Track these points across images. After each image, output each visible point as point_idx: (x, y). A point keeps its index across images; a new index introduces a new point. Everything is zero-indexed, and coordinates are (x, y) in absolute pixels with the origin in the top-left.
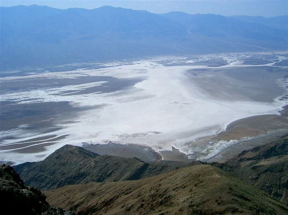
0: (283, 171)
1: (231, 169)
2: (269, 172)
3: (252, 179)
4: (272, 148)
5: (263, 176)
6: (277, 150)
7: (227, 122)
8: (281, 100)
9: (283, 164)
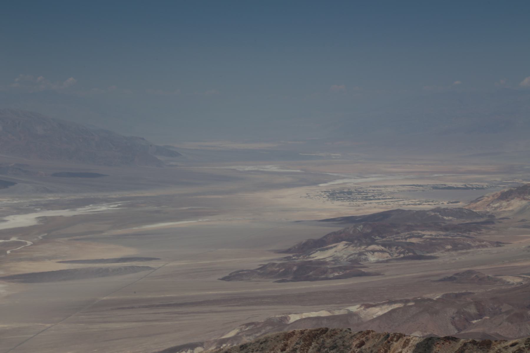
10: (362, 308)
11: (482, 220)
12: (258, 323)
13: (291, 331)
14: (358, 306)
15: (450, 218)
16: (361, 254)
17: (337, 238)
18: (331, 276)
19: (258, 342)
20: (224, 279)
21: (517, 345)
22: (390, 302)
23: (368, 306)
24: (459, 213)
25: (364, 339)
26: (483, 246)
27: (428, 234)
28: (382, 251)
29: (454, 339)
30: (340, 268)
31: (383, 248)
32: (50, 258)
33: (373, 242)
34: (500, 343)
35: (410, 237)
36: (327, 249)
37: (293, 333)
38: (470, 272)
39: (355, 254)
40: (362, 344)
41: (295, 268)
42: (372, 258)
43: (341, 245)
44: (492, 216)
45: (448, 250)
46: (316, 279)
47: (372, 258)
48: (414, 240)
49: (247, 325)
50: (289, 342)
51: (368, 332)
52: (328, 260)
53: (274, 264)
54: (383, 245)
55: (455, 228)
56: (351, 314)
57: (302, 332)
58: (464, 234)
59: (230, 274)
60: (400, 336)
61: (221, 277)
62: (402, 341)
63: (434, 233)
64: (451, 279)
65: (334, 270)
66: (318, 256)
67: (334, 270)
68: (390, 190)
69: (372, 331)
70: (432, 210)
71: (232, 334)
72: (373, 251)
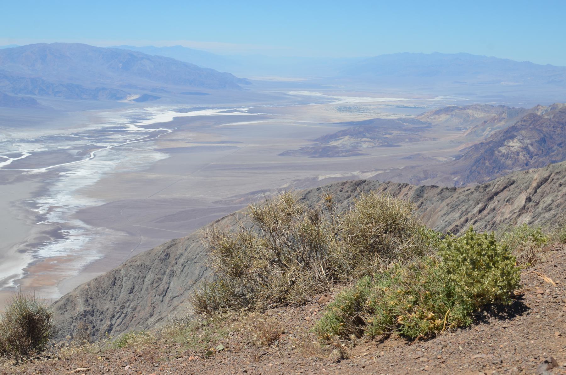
8: (22, 251)
10: (360, 173)
12: (301, 180)
13: (345, 181)
14: (358, 172)
15: (407, 124)
16: (358, 143)
17: (344, 133)
18: (341, 155)
19: (327, 186)
21: (470, 190)
23: (363, 172)
24: (412, 121)
25: (386, 186)
26: (426, 140)
27: (395, 132)
28: (370, 142)
29: (437, 187)
30: (346, 151)
31: (371, 140)
32: (182, 140)
33: (364, 136)
34: (461, 189)
35: (385, 134)
36: (339, 140)
37: (347, 182)
38: (419, 155)
39: (355, 143)
40: (386, 189)
41: (320, 150)
43: (347, 138)
44: (430, 124)
45: (407, 142)
46: (332, 156)
47: (365, 146)
48: (387, 136)
49: (295, 181)
50: (344, 187)
52: (339, 146)
53: (308, 147)
54: (371, 138)
55: (411, 130)
56: (354, 176)
57: (351, 182)
58: (415, 133)
59: (283, 152)
60: (407, 185)
61: (278, 154)
62: (408, 187)
63: (399, 132)
64: (409, 158)
65: (342, 152)
66: (333, 143)
67: (342, 152)
68: (372, 107)
69: (391, 182)
70: (398, 119)
72: (365, 142)
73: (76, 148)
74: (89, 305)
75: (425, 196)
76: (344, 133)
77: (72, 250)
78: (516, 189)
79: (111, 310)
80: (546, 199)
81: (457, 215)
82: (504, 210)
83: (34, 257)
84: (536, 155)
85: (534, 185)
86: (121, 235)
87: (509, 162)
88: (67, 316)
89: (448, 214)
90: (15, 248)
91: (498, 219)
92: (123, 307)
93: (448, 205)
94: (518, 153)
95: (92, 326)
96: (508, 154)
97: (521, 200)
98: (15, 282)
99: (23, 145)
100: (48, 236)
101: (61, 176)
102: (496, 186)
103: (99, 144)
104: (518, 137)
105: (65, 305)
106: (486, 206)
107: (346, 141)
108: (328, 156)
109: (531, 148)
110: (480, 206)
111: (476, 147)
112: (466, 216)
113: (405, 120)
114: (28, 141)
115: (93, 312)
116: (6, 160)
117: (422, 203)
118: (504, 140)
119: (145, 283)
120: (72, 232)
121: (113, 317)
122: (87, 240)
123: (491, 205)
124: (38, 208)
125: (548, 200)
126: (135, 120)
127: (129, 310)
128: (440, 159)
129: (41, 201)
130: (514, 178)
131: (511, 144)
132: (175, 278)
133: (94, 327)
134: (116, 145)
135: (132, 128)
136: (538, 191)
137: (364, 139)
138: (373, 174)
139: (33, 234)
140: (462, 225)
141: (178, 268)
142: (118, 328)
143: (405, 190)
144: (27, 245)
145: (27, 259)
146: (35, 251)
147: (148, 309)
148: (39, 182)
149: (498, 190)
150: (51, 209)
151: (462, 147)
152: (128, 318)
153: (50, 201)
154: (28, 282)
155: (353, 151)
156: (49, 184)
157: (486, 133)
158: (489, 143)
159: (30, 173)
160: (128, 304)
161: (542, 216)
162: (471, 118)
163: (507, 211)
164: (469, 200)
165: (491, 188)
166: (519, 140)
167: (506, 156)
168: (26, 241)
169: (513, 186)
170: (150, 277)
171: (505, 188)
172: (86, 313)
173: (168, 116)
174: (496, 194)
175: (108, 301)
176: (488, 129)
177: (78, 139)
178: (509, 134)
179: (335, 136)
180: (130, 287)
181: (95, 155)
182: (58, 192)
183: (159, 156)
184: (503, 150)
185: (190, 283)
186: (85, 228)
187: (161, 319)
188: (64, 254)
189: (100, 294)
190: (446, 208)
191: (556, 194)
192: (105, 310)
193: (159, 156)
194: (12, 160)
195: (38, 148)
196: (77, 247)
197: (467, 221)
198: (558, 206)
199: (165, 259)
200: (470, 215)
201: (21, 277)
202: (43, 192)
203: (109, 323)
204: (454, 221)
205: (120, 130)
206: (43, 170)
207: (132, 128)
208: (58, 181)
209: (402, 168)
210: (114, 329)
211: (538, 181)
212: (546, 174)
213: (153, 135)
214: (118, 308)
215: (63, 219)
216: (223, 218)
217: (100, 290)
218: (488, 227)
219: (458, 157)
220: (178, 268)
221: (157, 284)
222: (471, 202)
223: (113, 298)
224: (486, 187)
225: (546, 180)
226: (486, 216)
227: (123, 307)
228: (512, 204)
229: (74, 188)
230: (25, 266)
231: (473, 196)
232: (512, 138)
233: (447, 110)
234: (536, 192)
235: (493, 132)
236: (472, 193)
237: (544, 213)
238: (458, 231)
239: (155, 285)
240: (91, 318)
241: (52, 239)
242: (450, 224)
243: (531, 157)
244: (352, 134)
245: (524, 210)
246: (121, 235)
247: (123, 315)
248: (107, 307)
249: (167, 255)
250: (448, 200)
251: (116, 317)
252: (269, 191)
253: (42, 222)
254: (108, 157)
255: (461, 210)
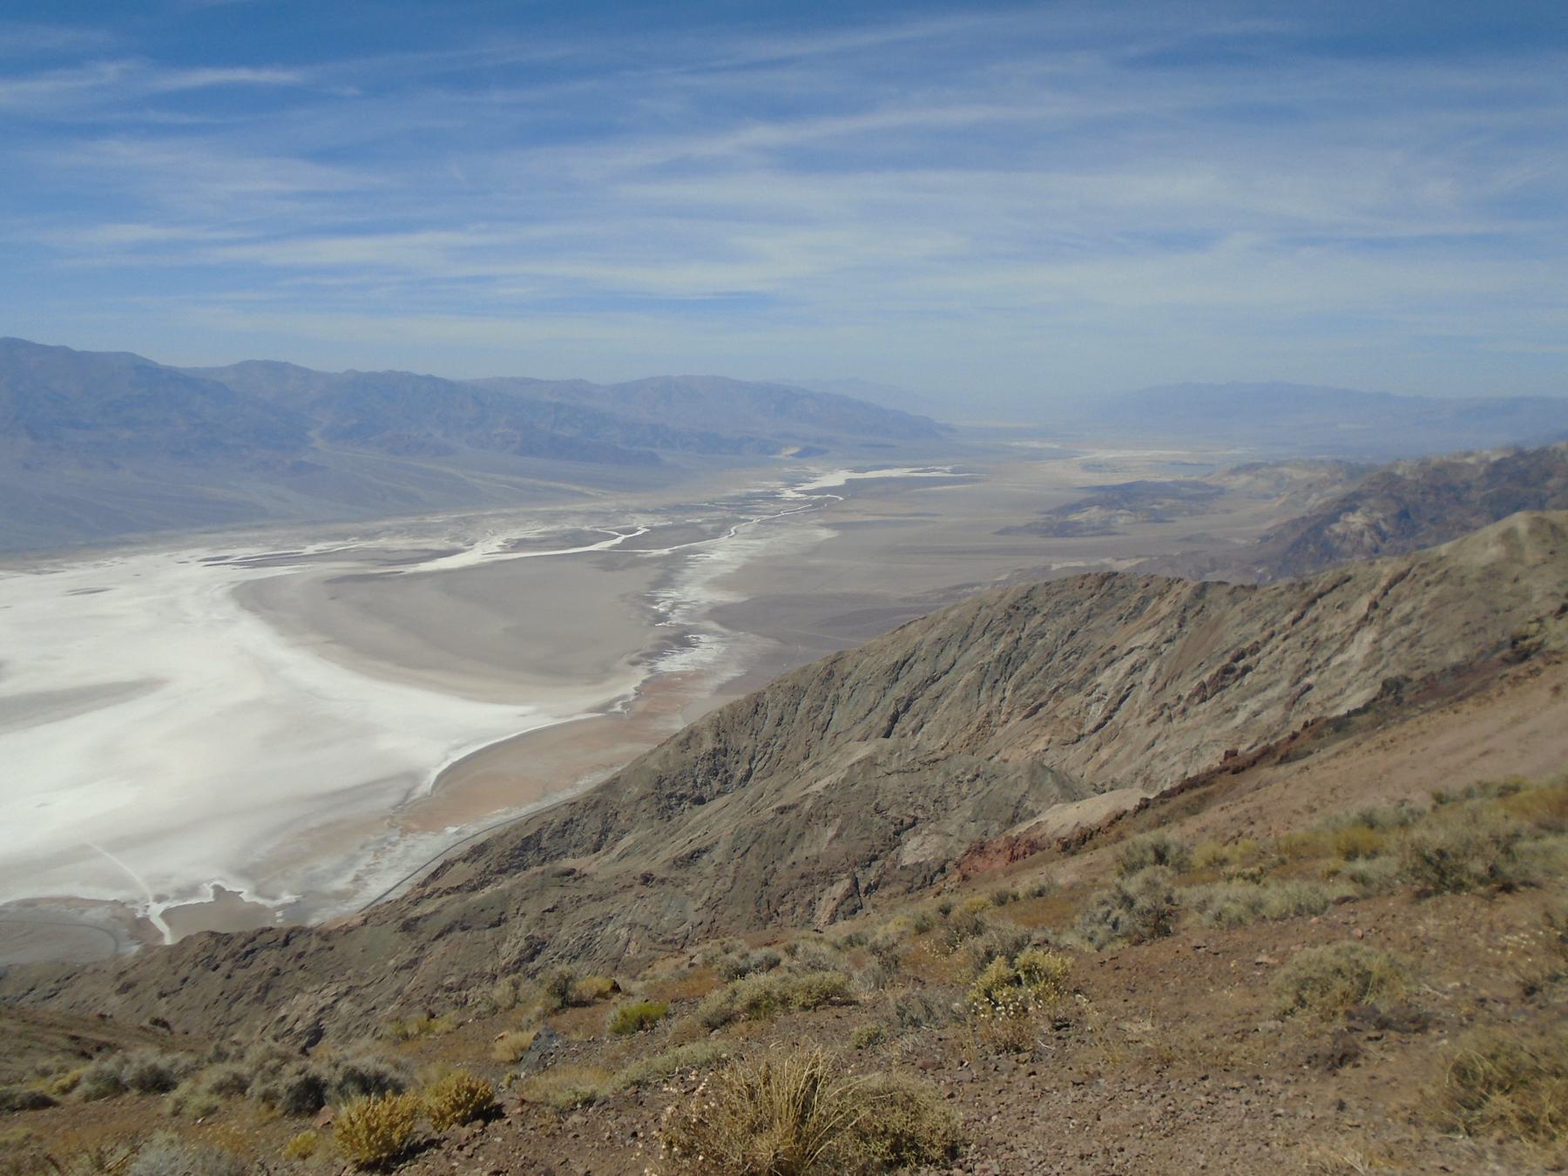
0: (505, 920)
1: (323, 944)
2: (457, 934)
3: (398, 969)
4: (528, 839)
5: (440, 947)
6: (544, 844)
7: (439, 765)
8: (634, 663)
9: (506, 898)
11: (1211, 491)
17: (1090, 503)
20: (995, 533)
22: (1138, 557)
23: (1118, 560)
24: (1195, 485)
27: (1168, 502)
29: (1225, 583)
30: (1094, 528)
33: (1121, 507)
37: (1089, 574)
40: (1147, 585)
42: (1121, 521)
43: (1094, 509)
47: (1121, 521)
48: (1156, 506)
49: (1017, 570)
51: (1152, 577)
56: (1103, 566)
62: (1181, 584)
64: (1189, 540)
70: (1174, 483)
71: (1004, 577)
72: (1121, 515)
73: (710, 522)
74: (720, 741)
75: (1208, 596)
76: (1090, 503)
77: (702, 663)
78: (1354, 590)
79: (750, 749)
80: (1402, 605)
81: (1258, 626)
82: (1332, 621)
83: (651, 671)
84: (1392, 536)
85: (1384, 583)
86: (770, 644)
87: (1347, 547)
88: (690, 754)
89: (1244, 625)
90: (625, 659)
91: (1323, 634)
92: (767, 745)
93: (1243, 611)
94: (1362, 534)
95: (723, 770)
96: (1345, 535)
97: (1361, 606)
98: (624, 706)
99: (638, 517)
100: (669, 642)
101: (689, 560)
102: (1320, 585)
103: (742, 517)
104: (1363, 509)
105: (688, 739)
106: (1302, 615)
107: (1094, 514)
108: (1066, 535)
109: (1384, 527)
110: (1294, 613)
111: (1294, 524)
112: (1271, 629)
113: (1182, 484)
114: (646, 512)
115: (726, 750)
116: (616, 537)
117: (1203, 607)
118: (1340, 513)
119: (799, 712)
120: (702, 638)
121: (753, 758)
122: (724, 648)
123: (1311, 614)
124: (658, 603)
125: (1406, 607)
126: (792, 483)
127: (776, 749)
128: (1237, 541)
129: (663, 594)
130: (1350, 573)
131: (1351, 519)
132: (841, 706)
133: (726, 771)
134: (765, 517)
135: (789, 494)
136: (1390, 592)
137: (1121, 511)
138: (1134, 562)
139: (650, 639)
140: (1266, 642)
141: (845, 692)
142: (760, 775)
143: (1177, 588)
144: (641, 655)
145: (641, 674)
146: (652, 664)
147: (802, 749)
148: (659, 568)
149: (1325, 590)
150: (674, 606)
151: (1271, 523)
152: (774, 759)
153: (674, 594)
154: (640, 706)
155: (1104, 529)
156: (673, 571)
157: (1311, 502)
158: (1316, 517)
159: (646, 556)
160: (774, 740)
161: (1396, 631)
162: (1287, 480)
163: (1336, 624)
164: (1277, 604)
165: (1313, 586)
166: (1365, 514)
167: (1344, 538)
168: (638, 651)
169: (1348, 584)
170: (805, 703)
171: (1335, 587)
172: (715, 753)
173: (838, 478)
174: (1321, 595)
175: (746, 736)
176: (1315, 496)
177: (714, 510)
178: (1349, 504)
179: (1077, 507)
180: (777, 717)
181: (735, 531)
182: (686, 582)
183: (825, 534)
184: (1338, 528)
185: (862, 714)
186: (722, 633)
187: (818, 764)
188: (691, 668)
189: (736, 725)
190: (1240, 616)
191: (1420, 597)
192: (742, 748)
193: (825, 534)
194: (623, 537)
195: (659, 522)
196: (708, 659)
197: (1272, 635)
198: (1422, 617)
199: (828, 679)
200: (1277, 627)
201: (632, 698)
202: (665, 582)
203: (748, 767)
204: (1252, 635)
205: (772, 497)
206: (666, 551)
207: (789, 494)
208: (686, 567)
209: (1177, 554)
210: (753, 775)
211: (1390, 576)
212: (1403, 567)
213: (817, 504)
214: (760, 745)
215: (690, 620)
216: (910, 623)
217: (736, 720)
218: (1307, 646)
219: (1265, 539)
220: (845, 692)
221: (815, 715)
222: (1279, 608)
223: (755, 732)
224: (1304, 585)
225: (1401, 577)
226: (1303, 629)
227: (767, 745)
228: (1347, 610)
229: (708, 577)
230: (638, 684)
231: (1283, 598)
232: (1353, 509)
233: (1250, 468)
234: (1386, 593)
235: (1321, 501)
236: (1282, 594)
237: (1399, 626)
238: (1258, 650)
239: (812, 715)
240: (723, 759)
241: (675, 647)
242: (1246, 639)
243: (1384, 540)
244: (1101, 504)
245: (1366, 620)
246: (770, 644)
247: (767, 756)
248: (744, 744)
249: (831, 674)
250: (1243, 605)
251: (757, 759)
252: (979, 584)
253: (664, 624)
254: (754, 535)
255: (1263, 620)
